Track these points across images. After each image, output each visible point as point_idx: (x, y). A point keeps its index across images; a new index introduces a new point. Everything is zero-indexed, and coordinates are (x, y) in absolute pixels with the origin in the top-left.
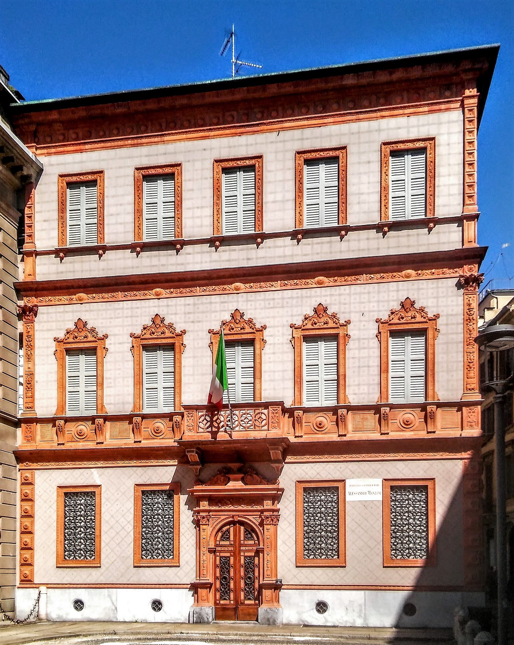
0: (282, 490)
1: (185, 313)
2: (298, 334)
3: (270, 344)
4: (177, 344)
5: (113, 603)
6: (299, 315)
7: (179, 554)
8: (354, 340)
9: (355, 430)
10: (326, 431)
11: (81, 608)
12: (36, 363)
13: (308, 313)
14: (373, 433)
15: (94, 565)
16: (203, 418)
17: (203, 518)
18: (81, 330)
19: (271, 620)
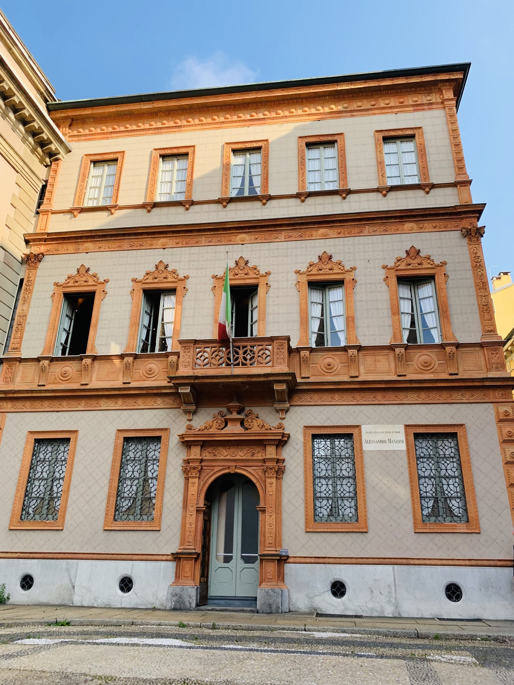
0: (289, 436)
1: (189, 261)
3: (275, 289)
5: (71, 580)
7: (161, 514)
9: (367, 372)
10: (336, 372)
11: (30, 587)
12: (31, 305)
13: (313, 260)
15: (55, 528)
17: (194, 468)
18: (82, 275)
19: (274, 607)
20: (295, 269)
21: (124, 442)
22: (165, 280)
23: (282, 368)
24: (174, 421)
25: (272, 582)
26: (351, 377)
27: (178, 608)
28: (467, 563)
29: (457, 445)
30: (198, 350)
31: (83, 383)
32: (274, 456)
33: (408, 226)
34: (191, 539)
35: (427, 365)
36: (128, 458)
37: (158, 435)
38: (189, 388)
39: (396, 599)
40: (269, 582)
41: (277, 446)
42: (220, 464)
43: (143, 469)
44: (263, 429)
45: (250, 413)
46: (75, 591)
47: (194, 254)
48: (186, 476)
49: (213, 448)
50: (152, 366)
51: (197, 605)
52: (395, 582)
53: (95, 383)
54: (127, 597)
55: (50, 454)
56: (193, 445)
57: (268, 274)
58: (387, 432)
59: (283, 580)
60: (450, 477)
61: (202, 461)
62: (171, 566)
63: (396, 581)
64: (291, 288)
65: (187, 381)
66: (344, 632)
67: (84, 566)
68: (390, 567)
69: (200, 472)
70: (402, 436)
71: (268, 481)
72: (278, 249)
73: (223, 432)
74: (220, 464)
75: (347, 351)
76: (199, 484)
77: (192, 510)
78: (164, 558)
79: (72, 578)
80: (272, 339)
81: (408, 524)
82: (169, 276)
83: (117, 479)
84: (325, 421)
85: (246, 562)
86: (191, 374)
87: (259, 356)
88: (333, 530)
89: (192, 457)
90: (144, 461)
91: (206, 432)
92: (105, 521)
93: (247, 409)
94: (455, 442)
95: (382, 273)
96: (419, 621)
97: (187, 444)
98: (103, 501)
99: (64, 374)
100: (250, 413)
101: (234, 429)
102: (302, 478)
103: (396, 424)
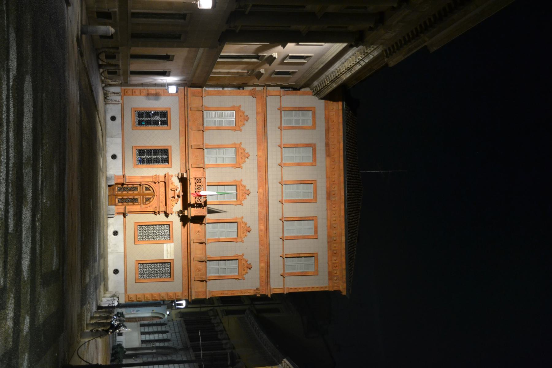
33: (263, 265)
67: (119, 140)
68: (123, 251)
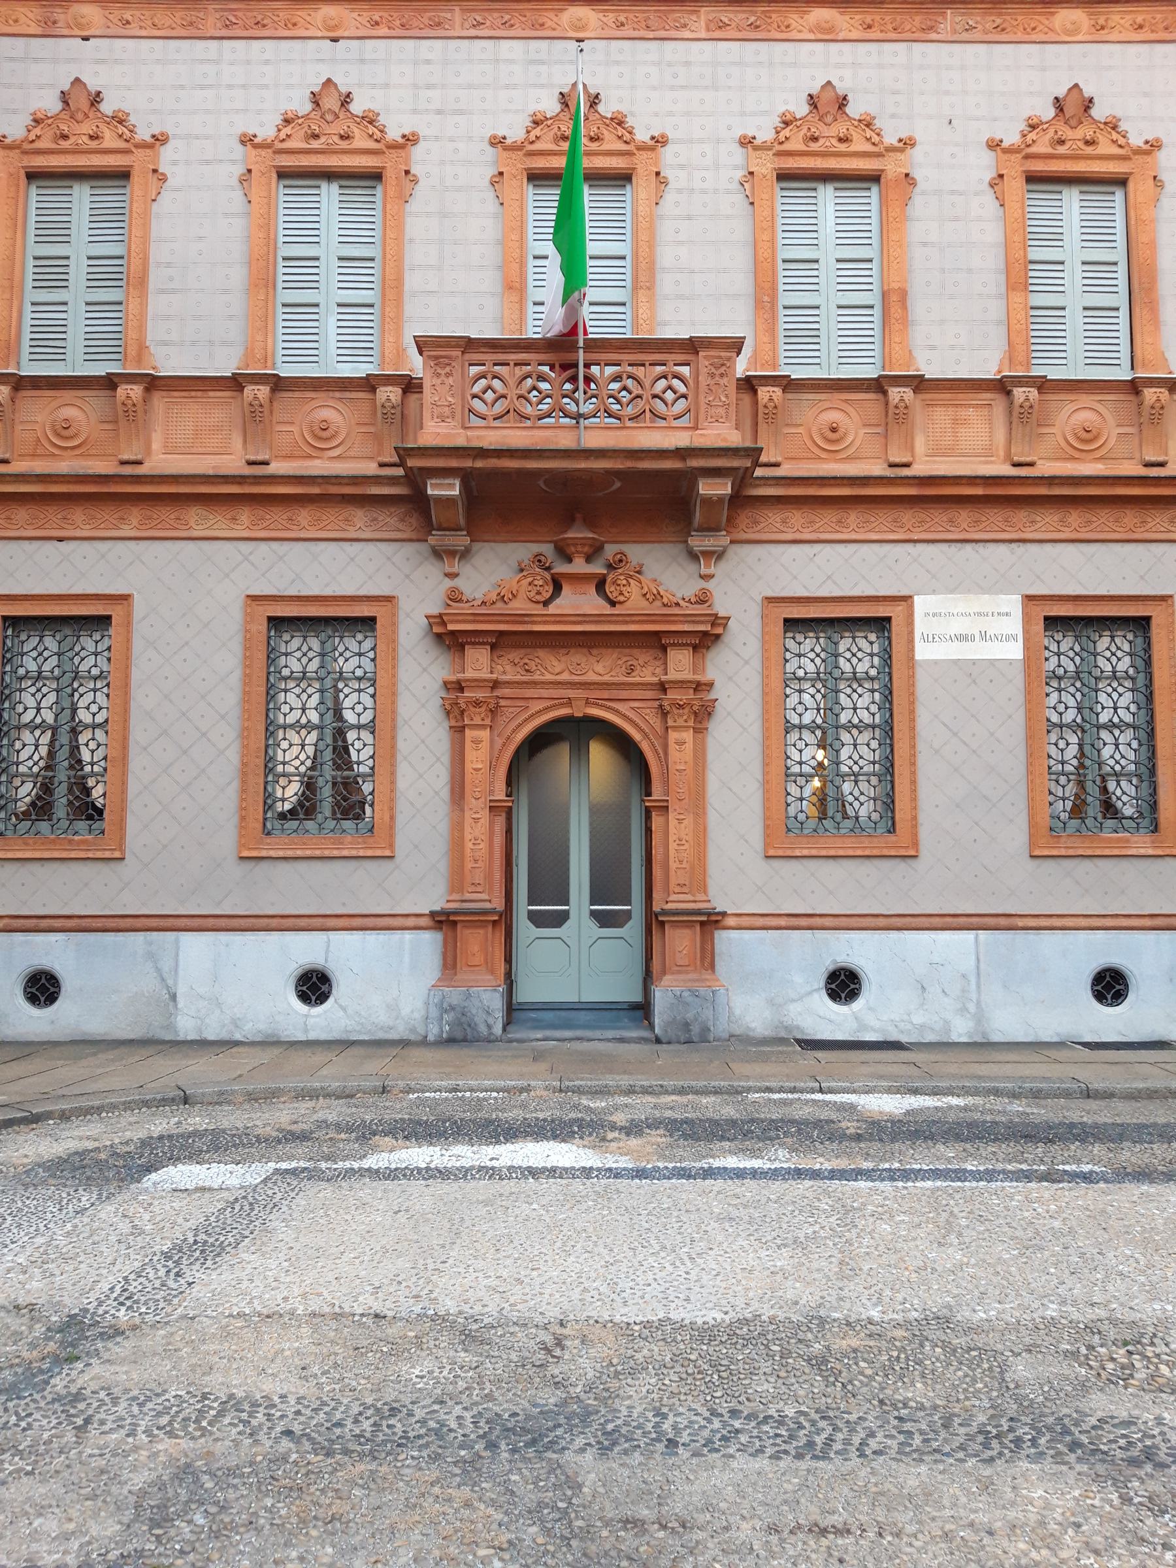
1: (416, 86)
2: (766, 166)
3: (680, 191)
4: (389, 175)
5: (163, 980)
6: (764, 113)
7: (392, 818)
8: (923, 193)
10: (850, 452)
11: (51, 999)
13: (792, 108)
14: (987, 463)
15: (99, 855)
16: (483, 383)
17: (477, 703)
19: (695, 1029)
20: (738, 133)
21: (269, 630)
22: (344, 145)
23: (722, 433)
24: (407, 576)
25: (687, 972)
26: (892, 465)
27: (460, 1037)
28: (1148, 922)
29: (1148, 648)
30: (474, 370)
31: (125, 457)
32: (687, 675)
34: (479, 877)
35: (1088, 435)
36: (286, 672)
37: (366, 614)
38: (457, 483)
39: (978, 1003)
40: (679, 972)
41: (695, 648)
42: (545, 693)
43: (330, 704)
44: (658, 603)
45: (621, 561)
46: (179, 1006)
47: (428, 62)
48: (453, 723)
49: (523, 651)
50: (326, 414)
51: (504, 1030)
52: (978, 968)
53: (161, 459)
54: (318, 1016)
55: (54, 661)
56: (469, 643)
57: (660, 141)
58: (979, 614)
59: (712, 967)
60: (1122, 726)
61: (496, 685)
62: (429, 942)
63: (982, 966)
64: (728, 192)
65: (454, 463)
66: (915, 1092)
67: (195, 947)
68: (969, 936)
69: (491, 710)
70: (1014, 625)
71: (673, 736)
72: (687, 64)
73: (552, 609)
74: (545, 693)
75: (885, 393)
76: (492, 741)
77: (477, 809)
78: (411, 922)
79: (165, 975)
80: (692, 346)
81: (1016, 835)
82: (356, 131)
83: (262, 727)
84: (820, 586)
85: (603, 925)
86: (461, 442)
87: (655, 396)
88: (832, 853)
89: (470, 674)
90: (328, 683)
91: (499, 608)
92: (241, 836)
93: (610, 550)
94: (1140, 640)
95: (983, 165)
96: (1054, 1054)
97: (450, 638)
98: (229, 784)
99: (64, 429)
100: (621, 561)
101: (579, 603)
102: (756, 730)
103: (1002, 592)
